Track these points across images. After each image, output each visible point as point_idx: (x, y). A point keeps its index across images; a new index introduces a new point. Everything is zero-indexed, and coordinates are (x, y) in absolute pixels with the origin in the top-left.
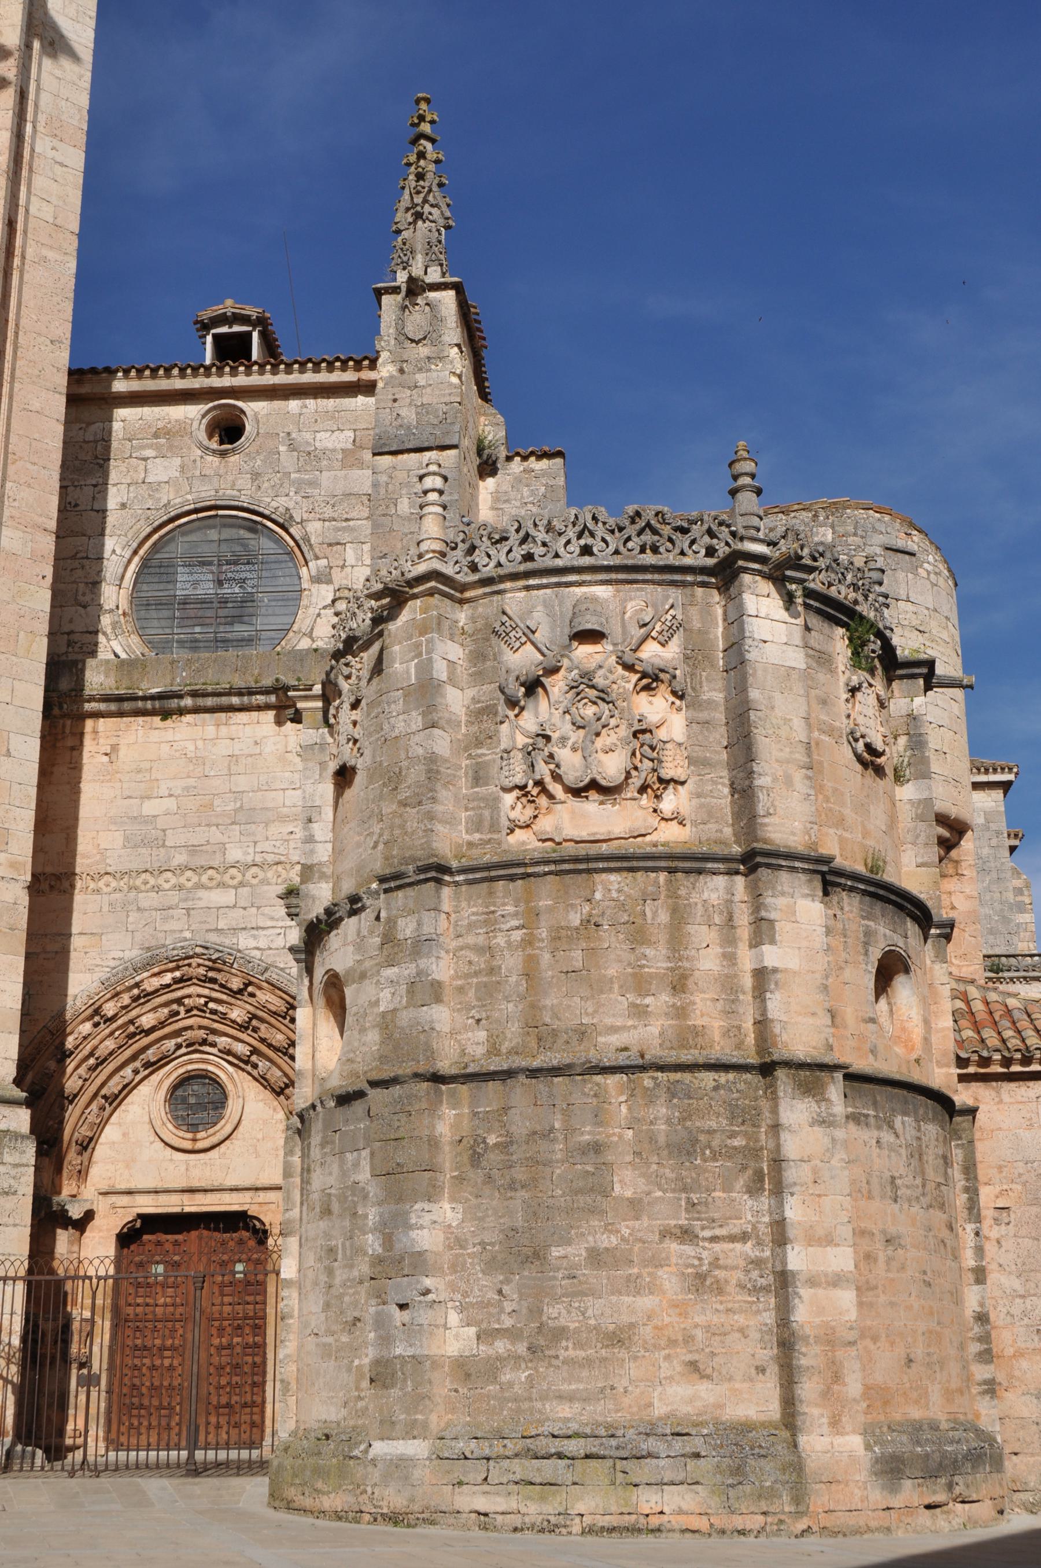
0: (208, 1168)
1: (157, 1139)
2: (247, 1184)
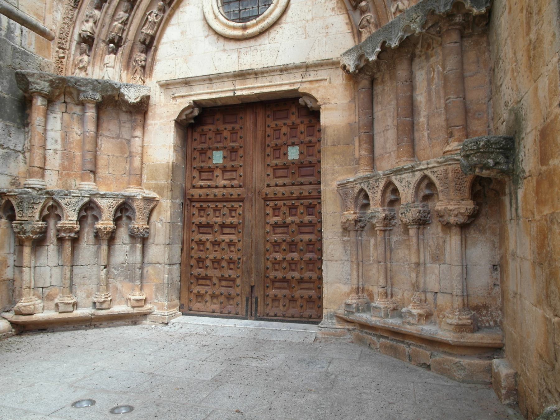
0: (259, 53)
1: (211, 33)
2: (297, 62)
